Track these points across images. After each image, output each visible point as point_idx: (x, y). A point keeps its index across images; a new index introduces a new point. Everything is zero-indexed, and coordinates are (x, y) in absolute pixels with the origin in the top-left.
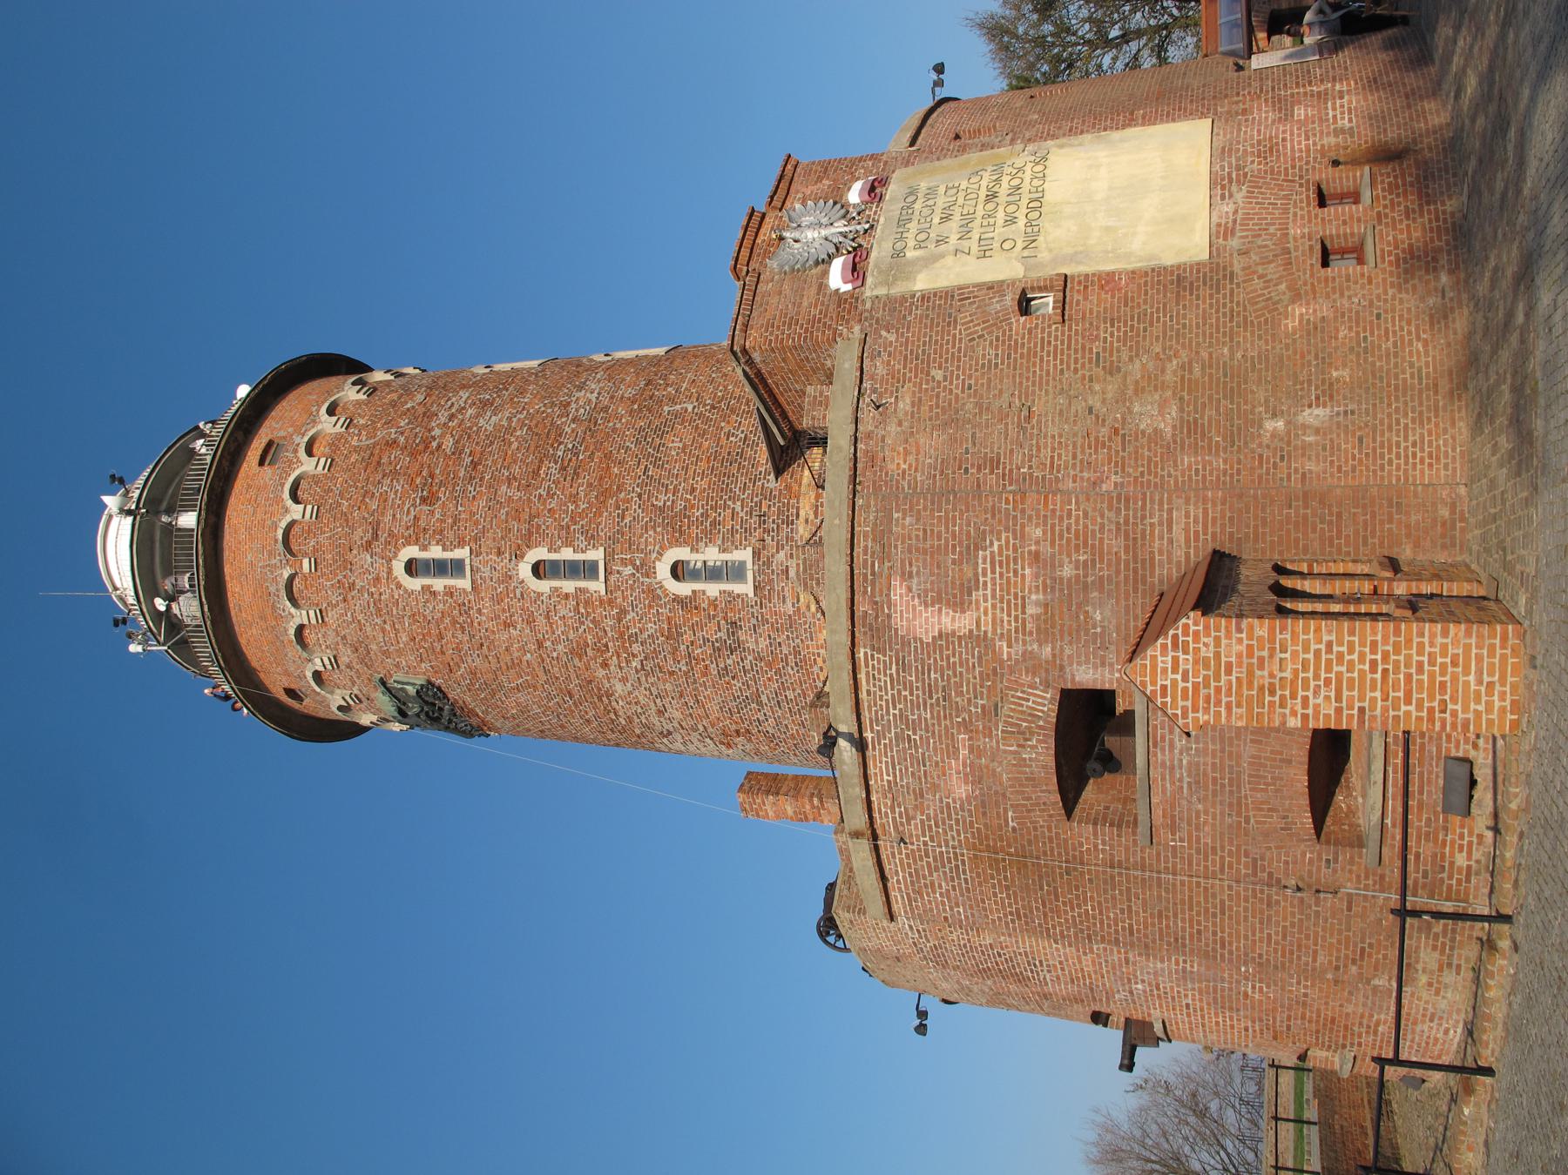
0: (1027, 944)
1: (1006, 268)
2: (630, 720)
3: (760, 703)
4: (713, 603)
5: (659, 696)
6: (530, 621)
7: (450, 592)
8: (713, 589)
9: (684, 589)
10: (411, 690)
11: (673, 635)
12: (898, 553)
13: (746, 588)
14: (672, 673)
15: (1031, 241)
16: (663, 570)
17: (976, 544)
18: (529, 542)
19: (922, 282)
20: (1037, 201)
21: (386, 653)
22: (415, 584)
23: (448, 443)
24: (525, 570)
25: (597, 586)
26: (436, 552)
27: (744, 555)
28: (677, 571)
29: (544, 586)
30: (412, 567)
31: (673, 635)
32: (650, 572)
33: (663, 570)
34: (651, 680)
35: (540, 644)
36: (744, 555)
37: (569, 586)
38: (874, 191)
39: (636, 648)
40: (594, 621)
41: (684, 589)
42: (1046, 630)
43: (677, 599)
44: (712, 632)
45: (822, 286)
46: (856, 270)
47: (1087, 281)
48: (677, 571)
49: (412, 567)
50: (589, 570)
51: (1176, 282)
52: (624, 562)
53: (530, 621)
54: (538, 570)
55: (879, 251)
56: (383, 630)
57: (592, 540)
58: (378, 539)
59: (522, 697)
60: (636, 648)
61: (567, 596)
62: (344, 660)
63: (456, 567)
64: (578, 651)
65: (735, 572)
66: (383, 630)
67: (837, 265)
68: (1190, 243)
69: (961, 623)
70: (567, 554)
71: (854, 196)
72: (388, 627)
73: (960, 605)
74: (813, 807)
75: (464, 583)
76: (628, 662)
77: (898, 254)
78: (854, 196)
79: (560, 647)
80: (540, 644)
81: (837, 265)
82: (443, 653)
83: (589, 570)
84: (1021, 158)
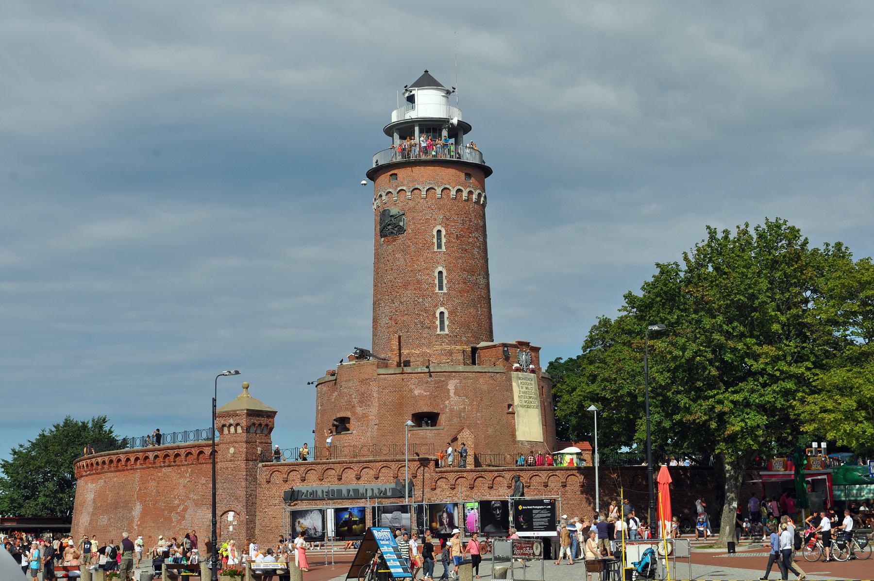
0: (376, 404)
1: (516, 401)
4: (434, 323)
6: (427, 268)
7: (433, 244)
8: (438, 323)
10: (401, 224)
11: (426, 311)
12: (464, 381)
13: (438, 332)
15: (522, 406)
16: (442, 309)
17: (466, 396)
18: (448, 270)
19: (514, 384)
20: (528, 407)
21: (413, 219)
22: (435, 233)
23: (471, 240)
24: (440, 269)
25: (437, 290)
26: (444, 240)
27: (446, 331)
28: (442, 313)
29: (436, 274)
30: (439, 231)
31: (426, 311)
32: (442, 305)
33: (442, 309)
36: (446, 331)
37: (437, 282)
38: (533, 371)
39: (421, 300)
41: (438, 315)
42: (452, 410)
43: (435, 313)
44: (427, 321)
45: (514, 362)
46: (517, 370)
47: (514, 418)
48: (442, 313)
49: (439, 231)
50: (441, 288)
51: (513, 435)
53: (427, 268)
54: (440, 273)
55: (520, 374)
57: (449, 289)
58: (446, 222)
60: (421, 300)
62: (410, 202)
63: (439, 246)
64: (419, 282)
65: (442, 329)
67: (518, 365)
68: (521, 436)
69: (452, 393)
70: (445, 282)
71: (531, 366)
73: (455, 394)
75: (436, 249)
77: (520, 378)
78: (531, 366)
81: (518, 365)
83: (441, 288)
84: (537, 403)
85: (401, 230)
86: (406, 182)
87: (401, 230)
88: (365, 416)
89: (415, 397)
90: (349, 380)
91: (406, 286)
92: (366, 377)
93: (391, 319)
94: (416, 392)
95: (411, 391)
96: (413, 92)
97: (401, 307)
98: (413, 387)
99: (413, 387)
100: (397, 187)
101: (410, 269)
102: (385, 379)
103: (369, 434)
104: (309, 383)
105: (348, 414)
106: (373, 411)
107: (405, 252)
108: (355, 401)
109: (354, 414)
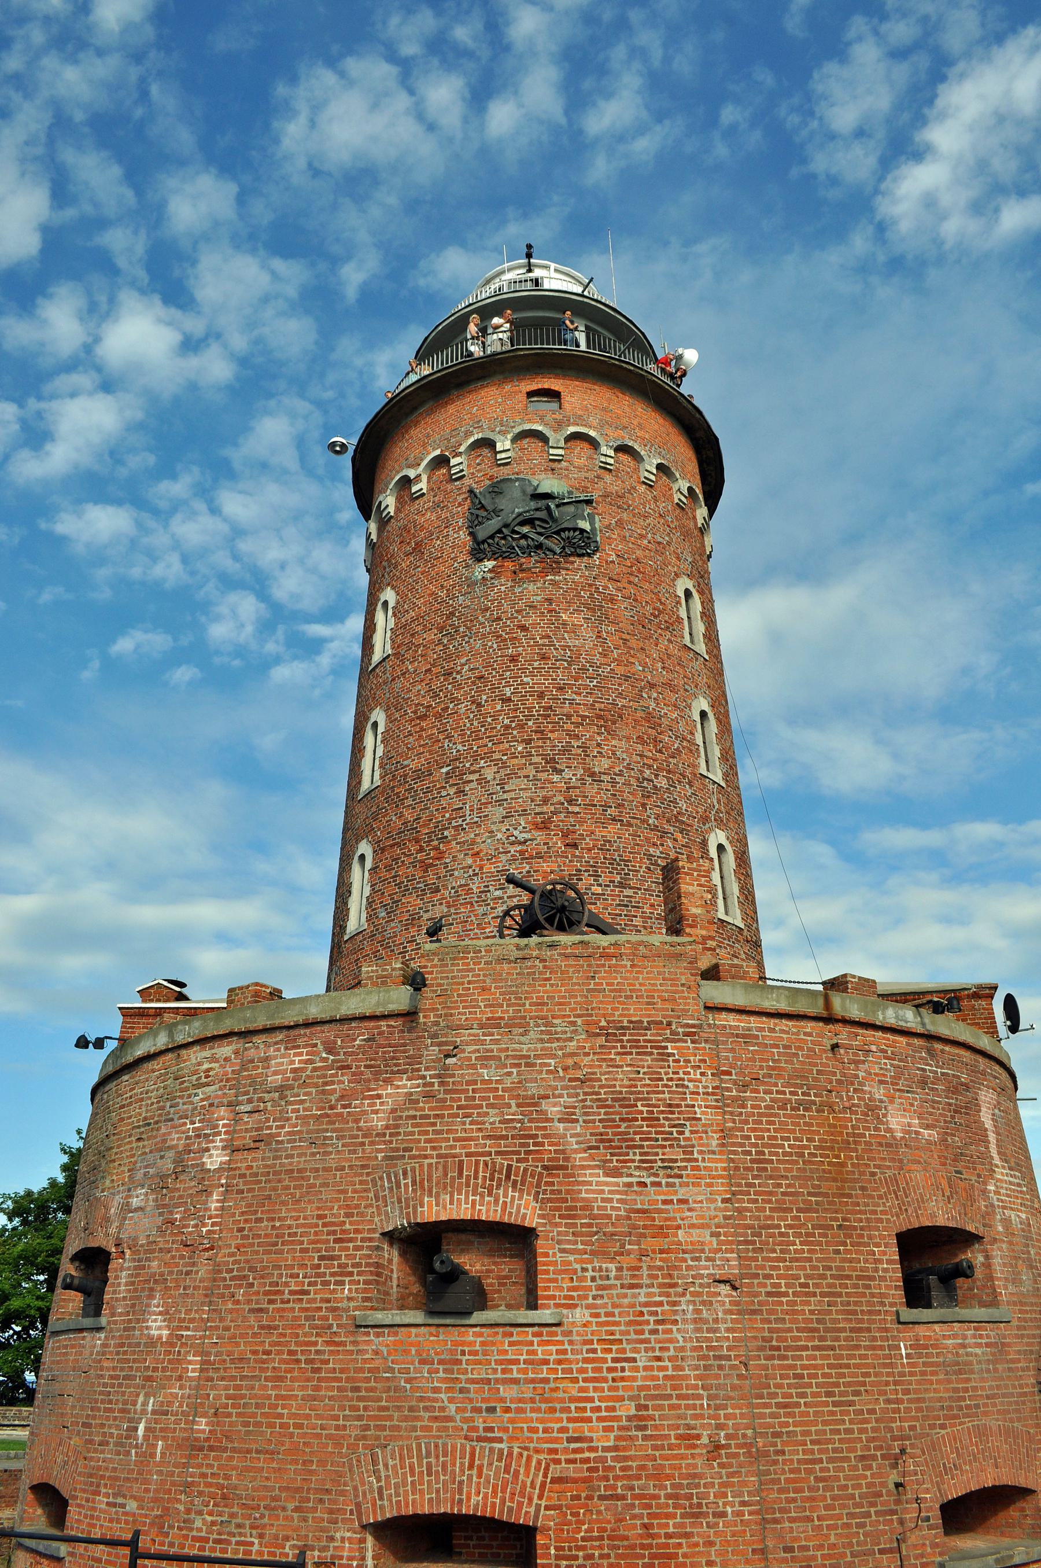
2: (577, 737)
3: (622, 885)
5: (614, 783)
6: (669, 685)
7: (679, 620)
9: (713, 853)
10: (585, 525)
14: (644, 805)
21: (620, 523)
34: (633, 781)
35: (652, 686)
39: (662, 782)
40: (677, 749)
43: (704, 843)
52: (719, 801)
53: (669, 685)
56: (642, 537)
59: (588, 634)
61: (692, 734)
62: (608, 478)
64: (651, 719)
66: (642, 537)
72: (645, 542)
74: (705, 939)
76: (650, 767)
79: (653, 705)
80: (652, 686)
82: (630, 582)
85: (582, 545)
86: (594, 420)
87: (582, 545)
88: (648, 1226)
89: (891, 1145)
90: (519, 1023)
91: (607, 720)
92: (635, 1012)
93: (544, 826)
94: (898, 1121)
95: (873, 1109)
96: (537, 273)
97: (591, 790)
98: (879, 1093)
99: (879, 1093)
100: (559, 426)
101: (620, 670)
102: (747, 1037)
103: (682, 1335)
104: (82, 1043)
105: (522, 1208)
106: (700, 1205)
107: (598, 609)
108: (572, 1137)
109: (566, 1207)
